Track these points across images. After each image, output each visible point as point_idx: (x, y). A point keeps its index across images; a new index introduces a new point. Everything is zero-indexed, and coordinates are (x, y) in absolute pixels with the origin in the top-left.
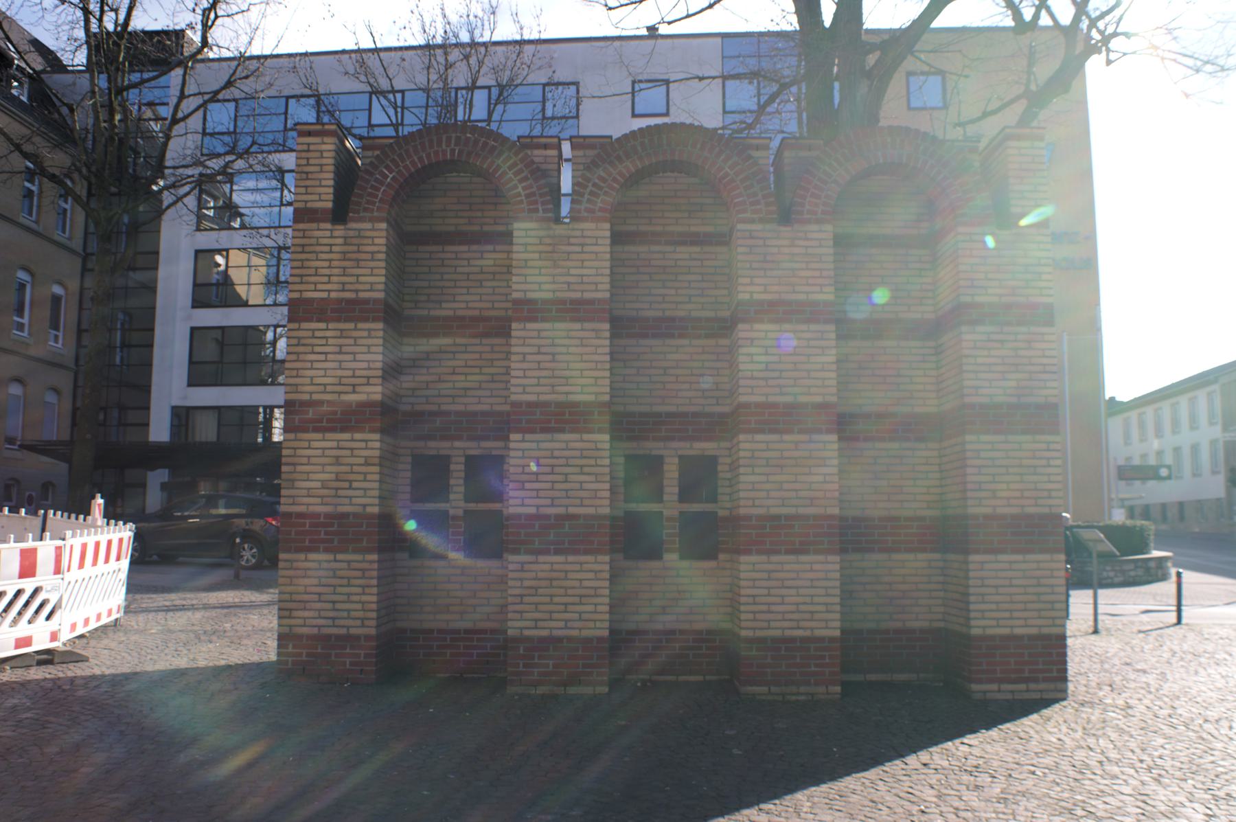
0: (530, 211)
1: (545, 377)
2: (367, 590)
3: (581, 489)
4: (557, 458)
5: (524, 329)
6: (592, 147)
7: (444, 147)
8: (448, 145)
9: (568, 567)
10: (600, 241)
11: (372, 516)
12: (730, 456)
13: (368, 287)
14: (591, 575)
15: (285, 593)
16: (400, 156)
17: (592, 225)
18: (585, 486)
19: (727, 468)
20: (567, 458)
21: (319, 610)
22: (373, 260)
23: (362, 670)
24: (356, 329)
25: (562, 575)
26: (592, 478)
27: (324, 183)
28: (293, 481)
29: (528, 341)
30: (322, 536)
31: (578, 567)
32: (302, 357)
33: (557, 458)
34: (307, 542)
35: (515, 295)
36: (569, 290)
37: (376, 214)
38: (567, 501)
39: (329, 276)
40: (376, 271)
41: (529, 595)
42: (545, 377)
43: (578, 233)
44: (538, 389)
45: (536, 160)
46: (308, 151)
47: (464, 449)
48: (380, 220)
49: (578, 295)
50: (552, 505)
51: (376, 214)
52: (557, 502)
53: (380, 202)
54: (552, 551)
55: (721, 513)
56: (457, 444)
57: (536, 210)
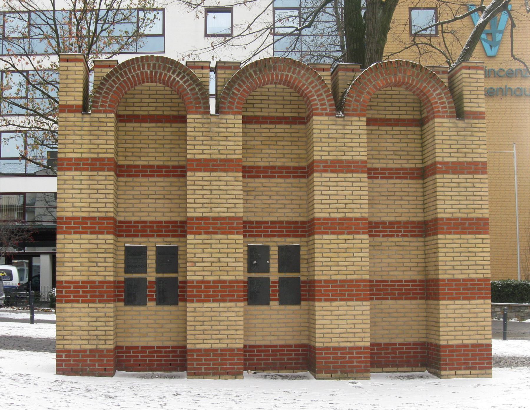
0: (196, 108)
1: (206, 203)
2: (107, 324)
3: (228, 266)
4: (214, 249)
5: (194, 176)
6: (229, 68)
7: (149, 71)
8: (149, 68)
9: (221, 309)
10: (236, 126)
11: (109, 282)
12: (307, 246)
13: (104, 151)
14: (234, 314)
15: (60, 326)
16: (121, 74)
17: (232, 117)
18: (230, 264)
19: (305, 253)
20: (219, 249)
21: (80, 335)
22: (107, 135)
23: (105, 369)
24: (98, 175)
25: (217, 314)
26: (234, 260)
27: (77, 90)
28: (64, 262)
29: (197, 183)
30: (81, 293)
31: (226, 309)
32: (67, 191)
33: (214, 249)
34: (72, 297)
35: (189, 156)
36: (219, 154)
37: (107, 108)
38: (219, 273)
39: (81, 144)
40: (108, 142)
41: (199, 325)
42: (206, 203)
43: (224, 121)
44: (202, 210)
45: (197, 76)
46: (67, 70)
47: (155, 243)
48: (111, 112)
49: (225, 156)
50: (211, 275)
51: (107, 108)
52: (214, 273)
53: (110, 101)
54: (212, 301)
55: (303, 278)
56: (151, 239)
57: (200, 108)
